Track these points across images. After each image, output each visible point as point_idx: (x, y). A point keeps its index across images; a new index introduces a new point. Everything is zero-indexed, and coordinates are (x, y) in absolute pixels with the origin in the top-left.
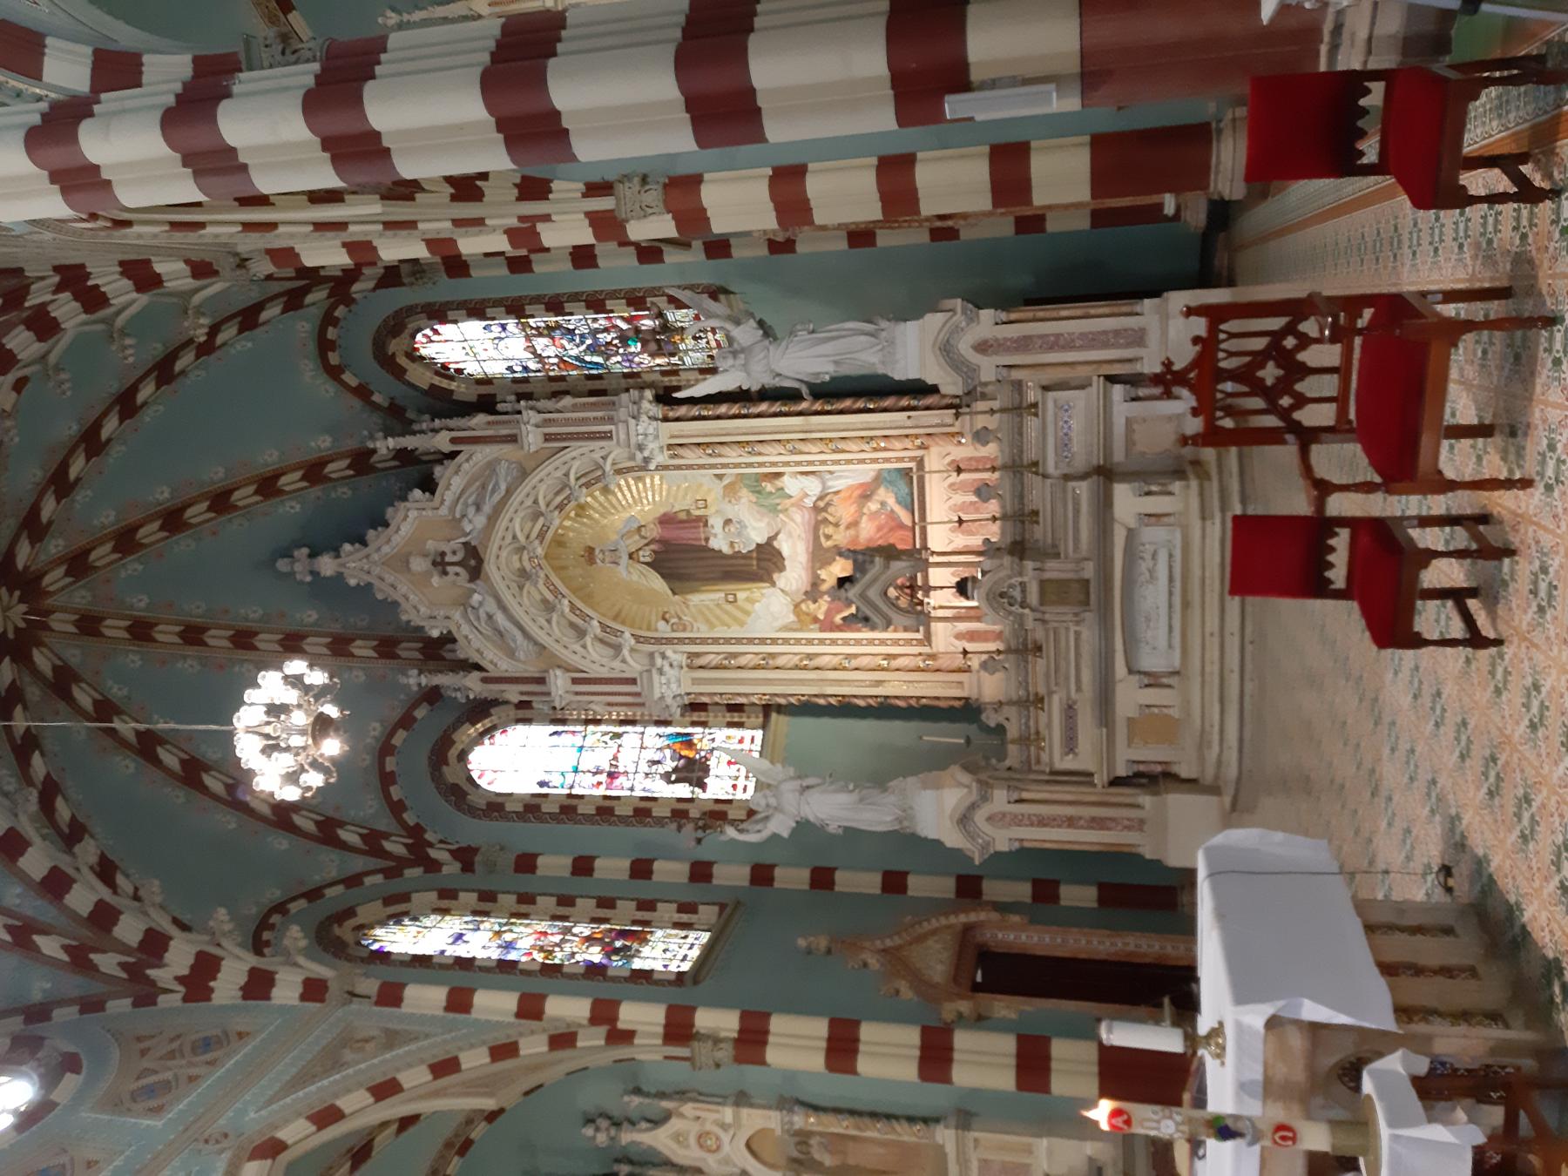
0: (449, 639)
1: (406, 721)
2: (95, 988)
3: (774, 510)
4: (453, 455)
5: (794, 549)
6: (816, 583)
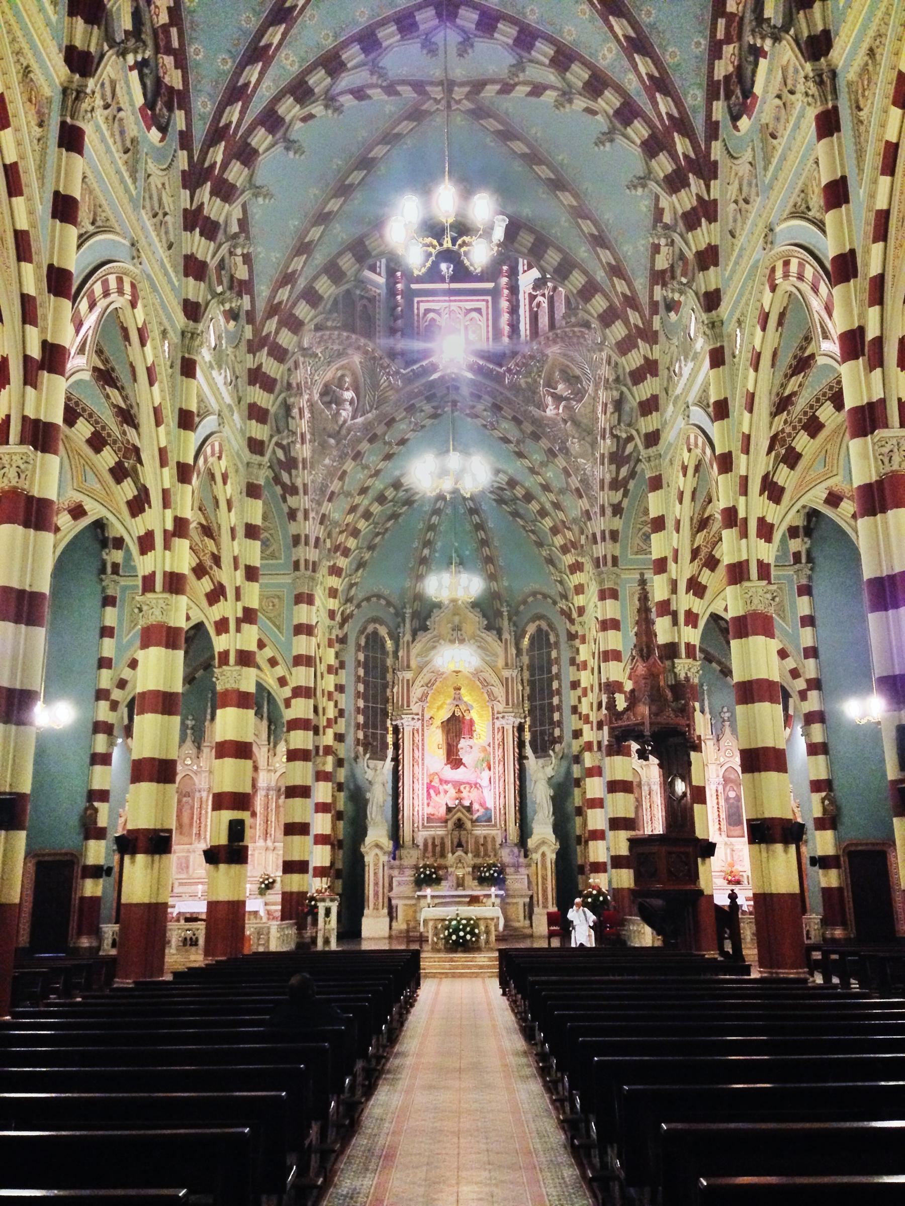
0: (425, 629)
1: (389, 604)
2: (334, 535)
3: (476, 767)
4: (501, 640)
5: (459, 774)
6: (447, 782)
